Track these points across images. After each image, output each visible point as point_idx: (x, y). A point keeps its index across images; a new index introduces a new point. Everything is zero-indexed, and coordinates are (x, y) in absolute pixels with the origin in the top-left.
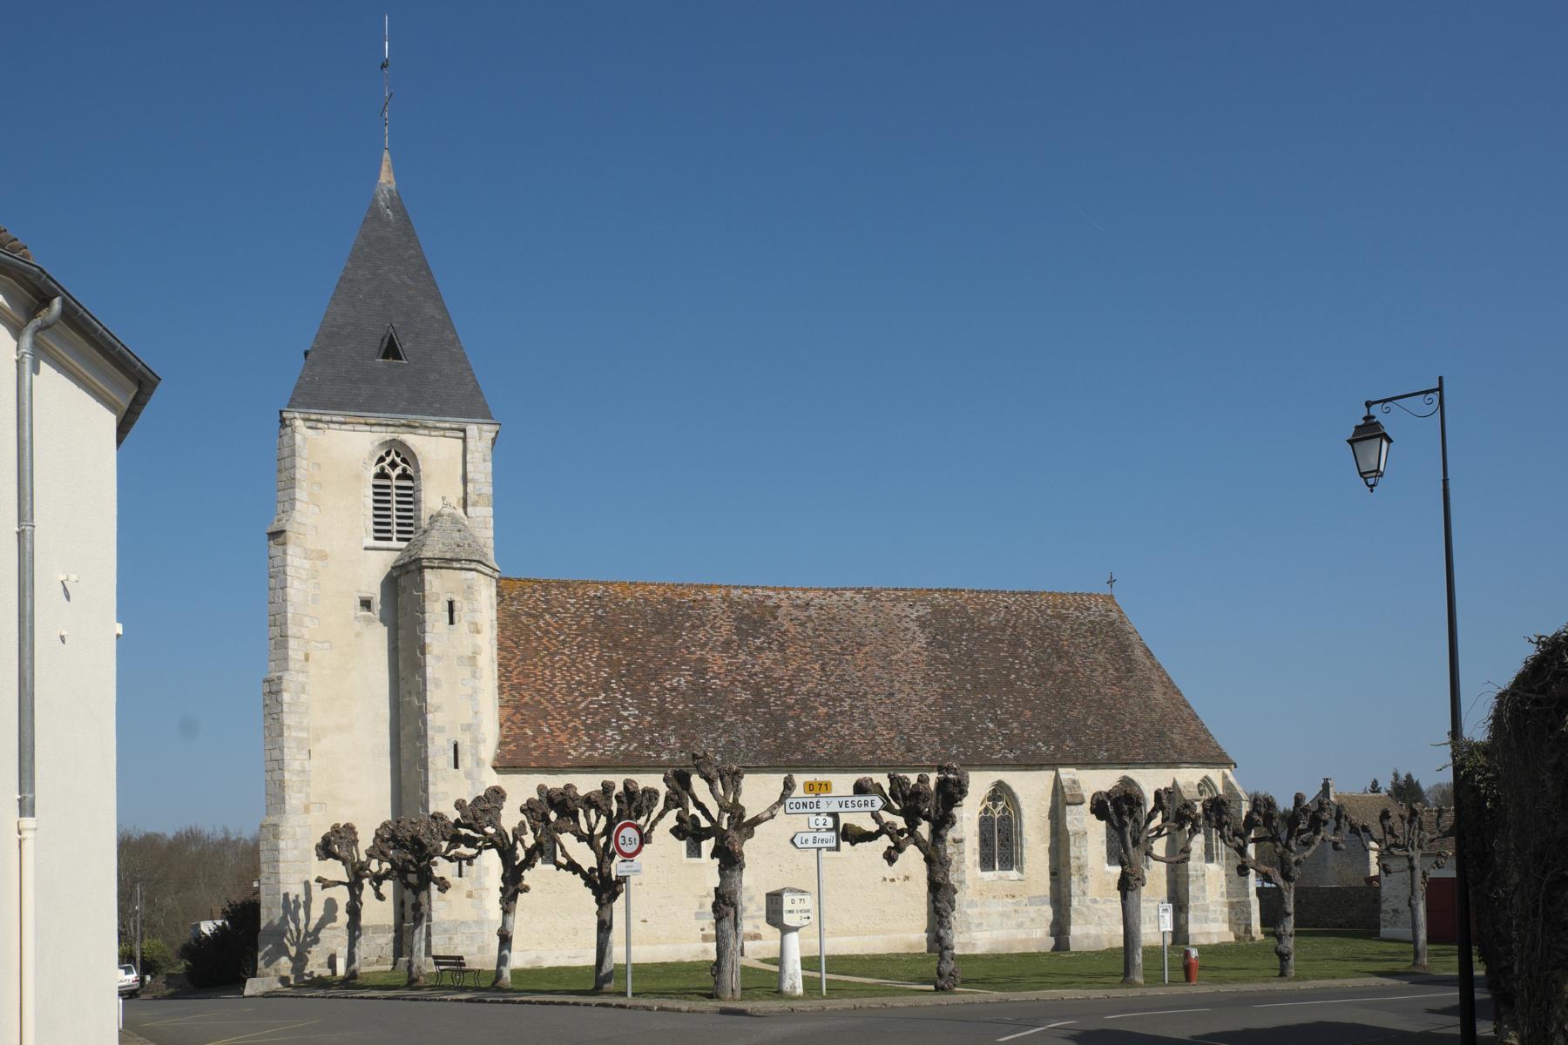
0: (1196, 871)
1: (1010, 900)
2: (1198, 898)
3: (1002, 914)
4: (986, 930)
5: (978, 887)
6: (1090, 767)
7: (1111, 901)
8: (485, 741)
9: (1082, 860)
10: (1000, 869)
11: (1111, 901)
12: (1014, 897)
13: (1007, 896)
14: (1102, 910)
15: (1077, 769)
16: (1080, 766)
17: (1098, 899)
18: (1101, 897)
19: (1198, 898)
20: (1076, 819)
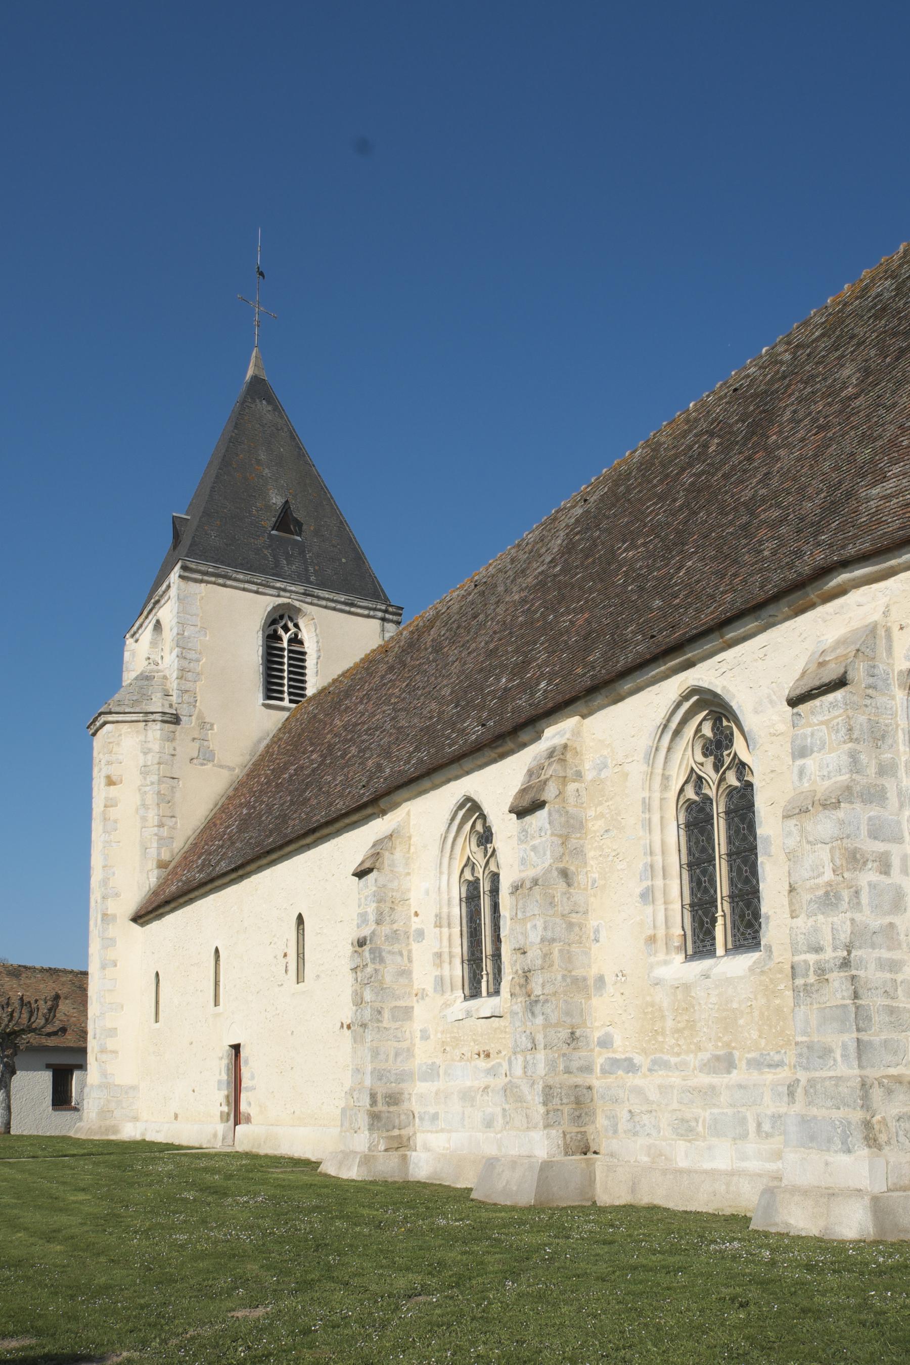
0: (818, 949)
1: (482, 1064)
2: (827, 1052)
3: (467, 1096)
4: (442, 1130)
5: (439, 1035)
6: (599, 699)
7: (666, 1065)
8: (117, 895)
9: (530, 954)
10: (489, 995)
11: (666, 1065)
12: (488, 1056)
13: (479, 1055)
14: (638, 1091)
15: (584, 717)
16: (580, 706)
17: (638, 1059)
18: (644, 1051)
19: (827, 1052)
20: (534, 848)
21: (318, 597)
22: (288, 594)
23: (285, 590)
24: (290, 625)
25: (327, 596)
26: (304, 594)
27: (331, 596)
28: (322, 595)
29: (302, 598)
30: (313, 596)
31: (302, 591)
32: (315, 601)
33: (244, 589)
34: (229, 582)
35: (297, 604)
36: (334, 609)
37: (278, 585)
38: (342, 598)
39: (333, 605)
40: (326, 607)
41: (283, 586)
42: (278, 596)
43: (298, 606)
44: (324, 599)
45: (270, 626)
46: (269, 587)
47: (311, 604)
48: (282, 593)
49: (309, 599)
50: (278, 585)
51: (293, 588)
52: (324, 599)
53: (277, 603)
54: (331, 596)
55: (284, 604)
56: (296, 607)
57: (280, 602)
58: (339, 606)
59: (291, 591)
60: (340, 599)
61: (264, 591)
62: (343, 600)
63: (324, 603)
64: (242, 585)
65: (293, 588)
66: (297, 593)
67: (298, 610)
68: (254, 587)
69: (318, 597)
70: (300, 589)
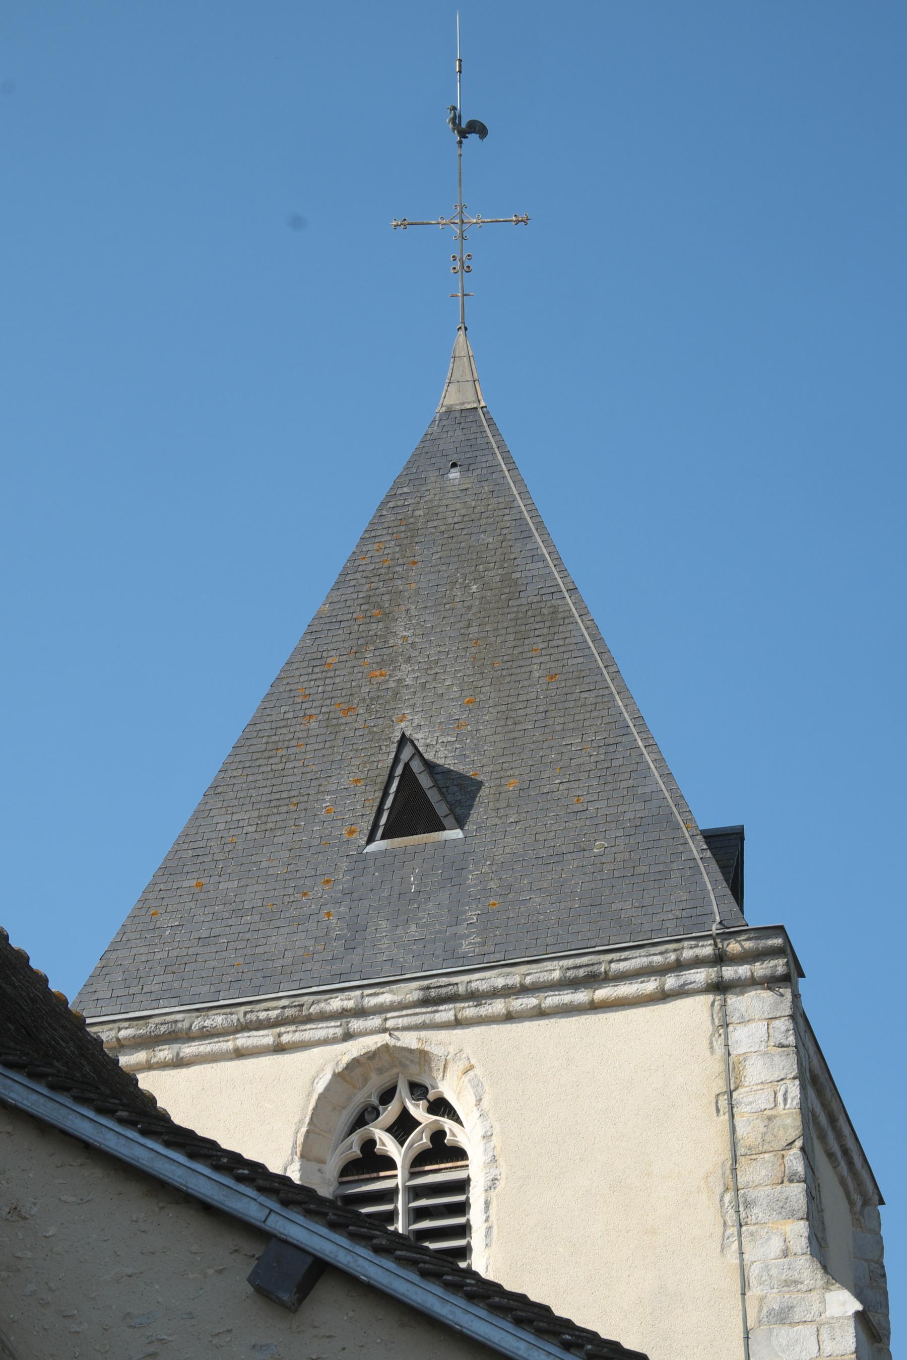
21: (475, 997)
22: (375, 1022)
23: (361, 1012)
24: (418, 1111)
25: (500, 982)
26: (425, 1002)
27: (514, 977)
28: (483, 986)
29: (424, 1015)
30: (453, 998)
31: (416, 996)
32: (469, 1011)
33: (239, 1054)
34: (189, 1050)
35: (410, 1040)
36: (541, 1013)
37: (336, 1004)
38: (554, 971)
39: (530, 1002)
40: (509, 1017)
41: (350, 1004)
42: (348, 1036)
43: (414, 1045)
44: (494, 994)
45: (352, 1131)
46: (309, 1019)
47: (458, 1023)
48: (356, 1024)
49: (446, 1013)
50: (336, 1004)
51: (386, 997)
52: (494, 994)
53: (345, 1060)
54: (514, 977)
55: (371, 1056)
56: (411, 1051)
57: (355, 1054)
58: (552, 1000)
59: (381, 1010)
60: (545, 977)
61: (297, 1037)
62: (556, 975)
63: (498, 1006)
64: (227, 1045)
65: (386, 997)
66: (401, 1006)
67: (423, 1057)
68: (265, 1038)
69: (475, 997)
70: (410, 992)
